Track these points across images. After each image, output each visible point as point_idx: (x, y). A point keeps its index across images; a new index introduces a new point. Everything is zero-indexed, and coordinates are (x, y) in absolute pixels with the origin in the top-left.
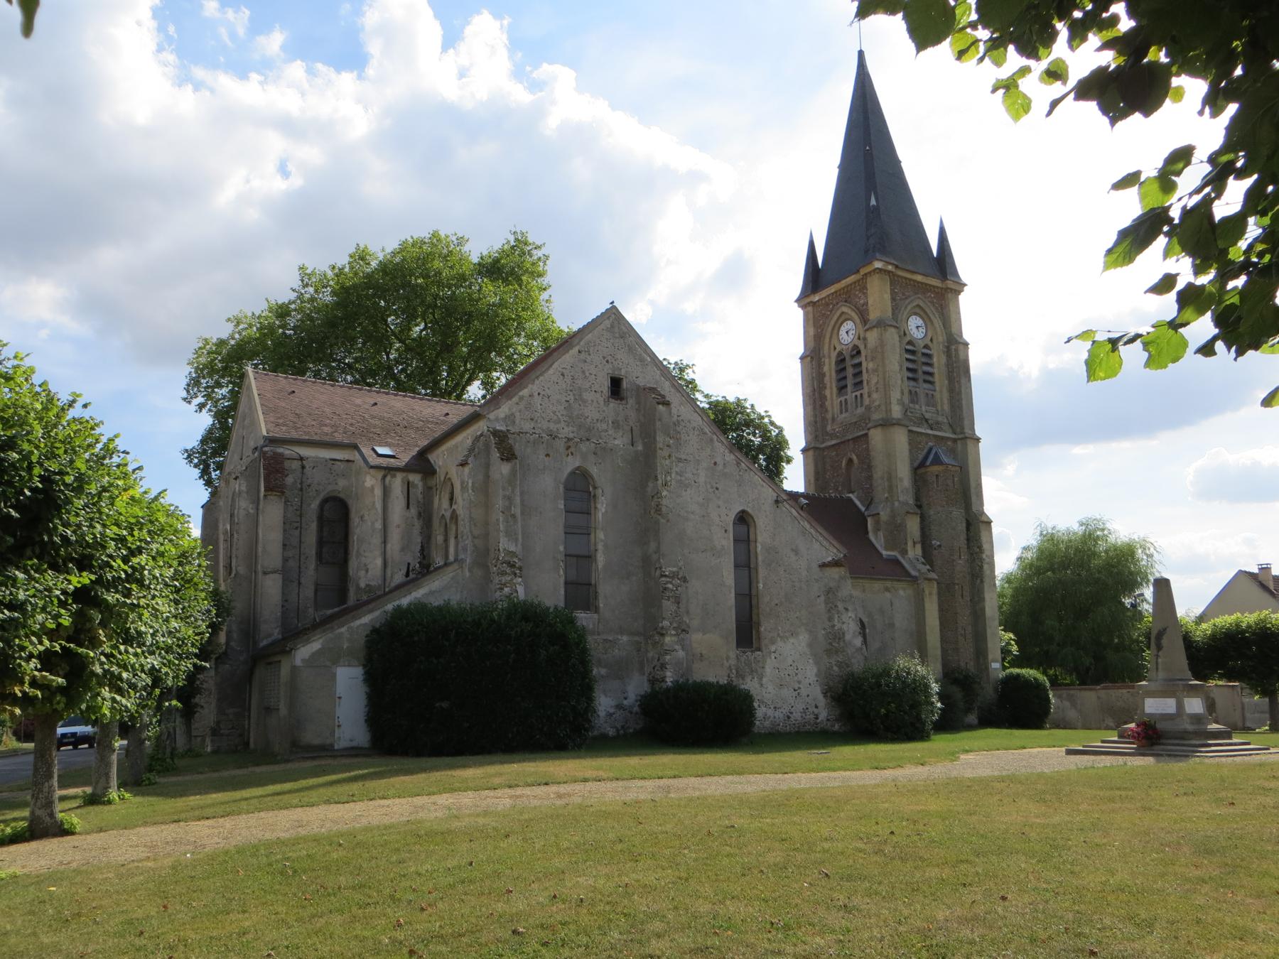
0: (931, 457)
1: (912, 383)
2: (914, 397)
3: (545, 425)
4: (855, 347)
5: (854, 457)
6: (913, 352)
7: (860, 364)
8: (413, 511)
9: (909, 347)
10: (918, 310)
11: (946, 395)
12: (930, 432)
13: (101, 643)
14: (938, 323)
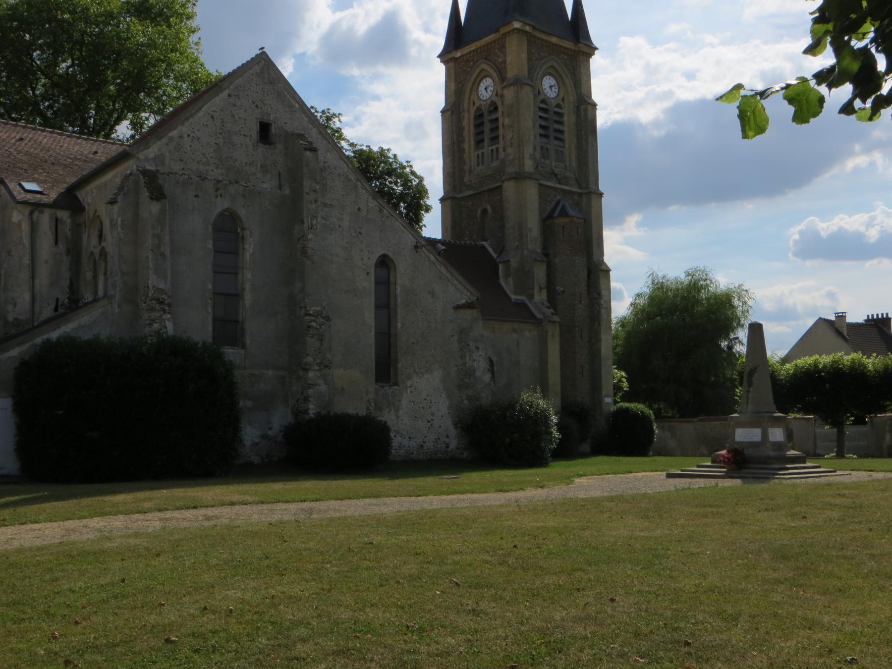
1: (544, 140)
2: (545, 151)
7: (497, 120)
8: (62, 247)
9: (541, 105)
12: (558, 186)
14: (569, 82)
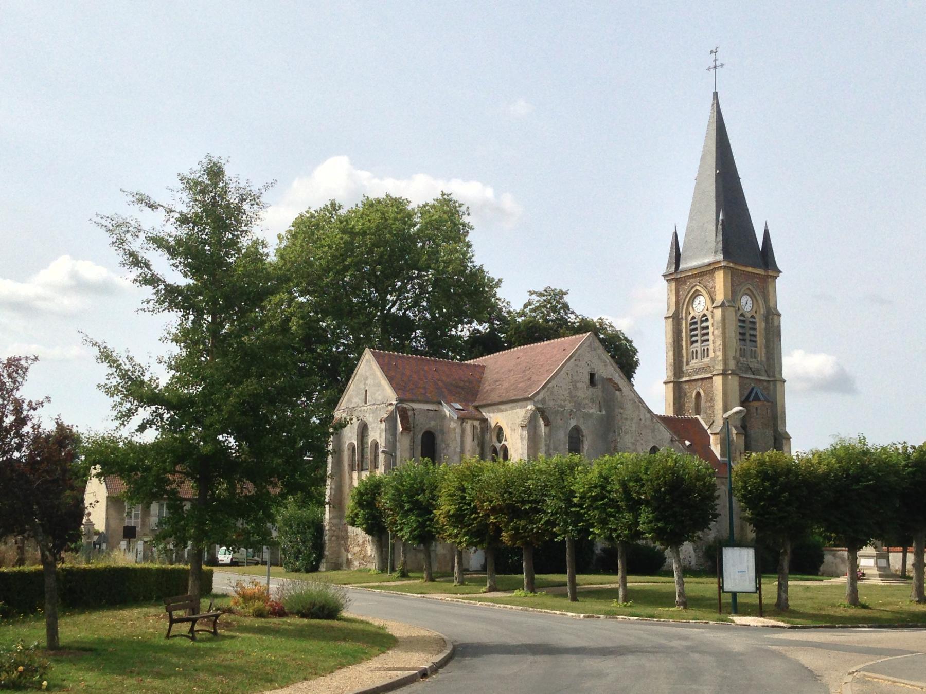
0: (753, 395)
1: (743, 342)
2: (743, 353)
3: (559, 402)
4: (704, 315)
5: (702, 392)
6: (743, 321)
7: (707, 328)
8: (476, 441)
9: (742, 318)
10: (748, 292)
11: (764, 351)
12: (752, 376)
13: (654, 539)
14: (761, 302)
